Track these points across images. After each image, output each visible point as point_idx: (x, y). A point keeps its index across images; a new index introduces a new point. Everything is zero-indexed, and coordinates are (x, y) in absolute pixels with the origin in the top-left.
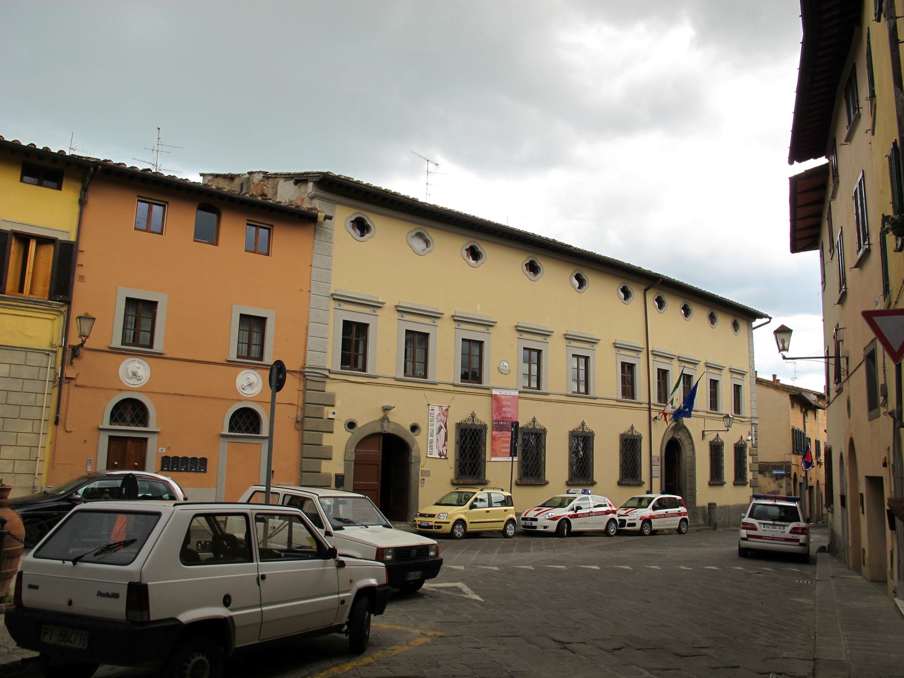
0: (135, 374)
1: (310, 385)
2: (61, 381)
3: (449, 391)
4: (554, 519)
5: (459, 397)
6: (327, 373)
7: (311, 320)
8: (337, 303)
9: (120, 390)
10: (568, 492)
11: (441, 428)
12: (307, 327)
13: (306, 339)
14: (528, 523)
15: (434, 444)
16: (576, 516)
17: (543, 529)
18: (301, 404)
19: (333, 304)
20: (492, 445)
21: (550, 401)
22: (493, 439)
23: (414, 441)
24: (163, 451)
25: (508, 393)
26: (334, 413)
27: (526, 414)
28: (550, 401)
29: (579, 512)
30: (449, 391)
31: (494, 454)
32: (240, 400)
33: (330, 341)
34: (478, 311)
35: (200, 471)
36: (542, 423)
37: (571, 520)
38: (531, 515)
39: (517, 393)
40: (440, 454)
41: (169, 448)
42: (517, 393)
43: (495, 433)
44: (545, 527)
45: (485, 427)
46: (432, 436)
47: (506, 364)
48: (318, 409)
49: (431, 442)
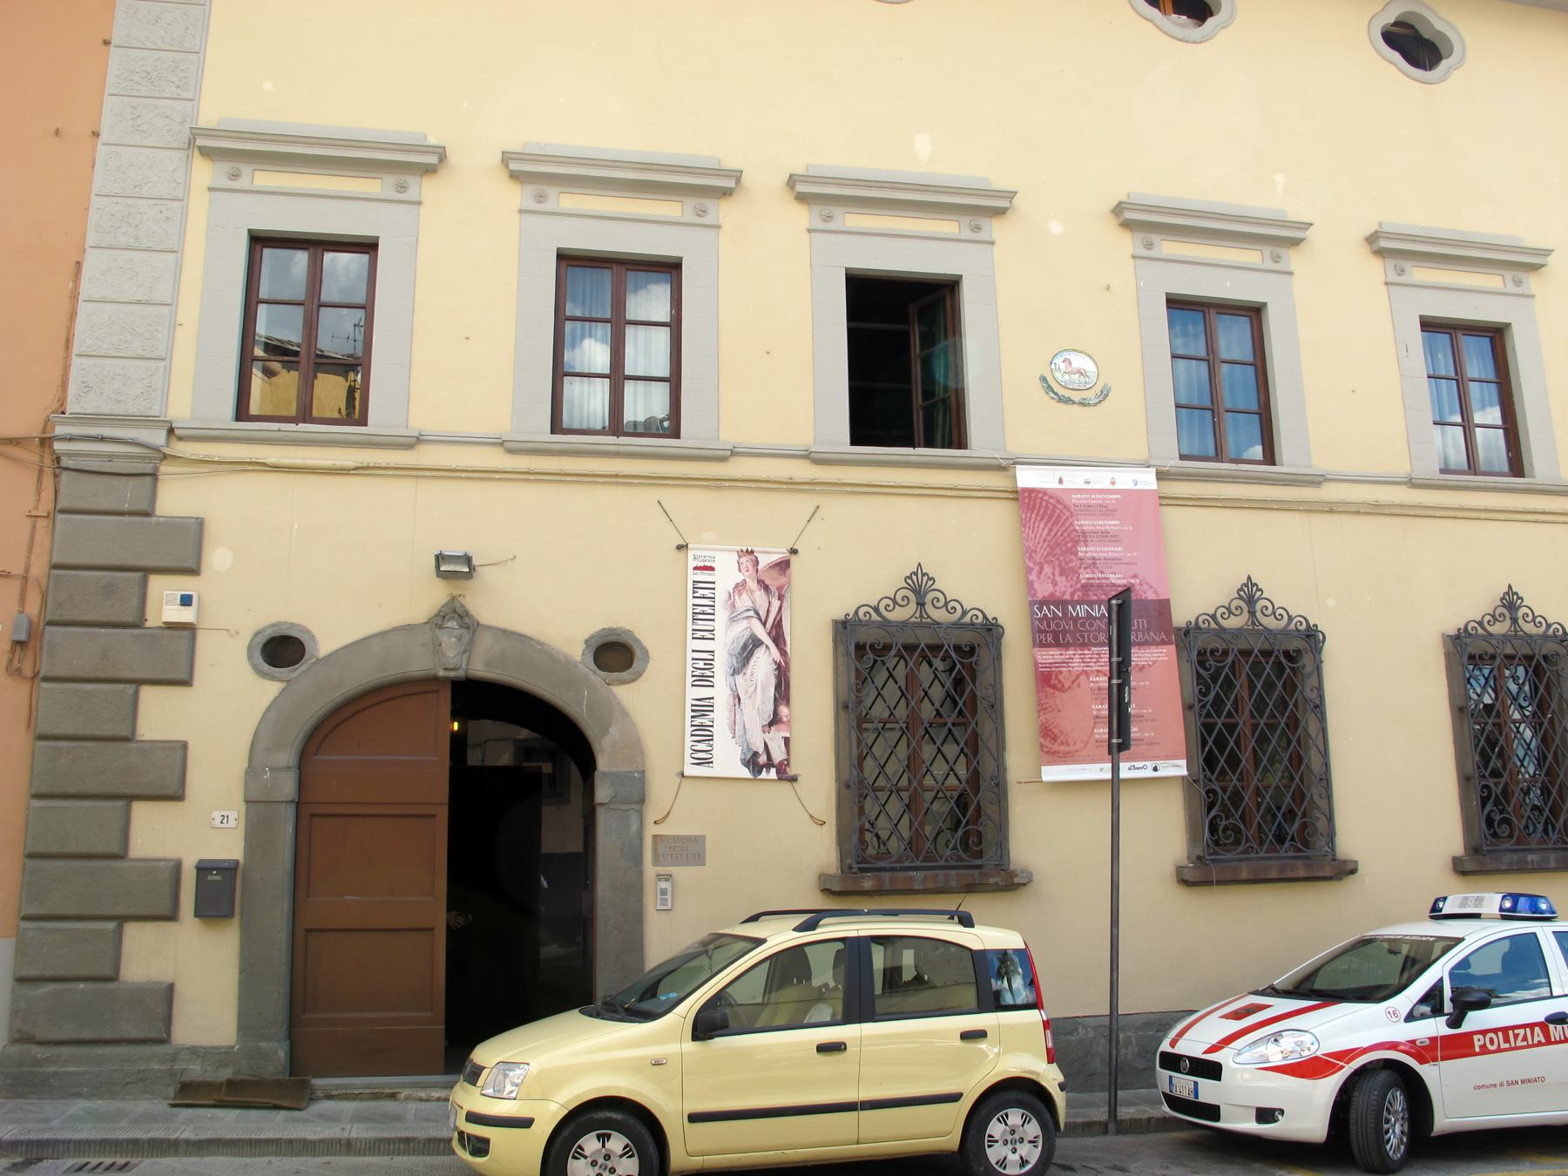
1: (75, 491)
3: (791, 485)
4: (1312, 1068)
5: (838, 510)
6: (158, 437)
7: (92, 238)
10: (1436, 914)
11: (749, 648)
12: (79, 264)
13: (73, 314)
14: (1183, 1084)
15: (720, 717)
16: (1457, 1047)
17: (1250, 1126)
18: (39, 569)
19: (204, 173)
20: (1042, 708)
21: (1331, 509)
22: (1046, 680)
23: (611, 712)
25: (1100, 479)
26: (186, 601)
27: (1208, 562)
28: (1331, 509)
29: (1475, 1020)
30: (791, 485)
31: (1053, 745)
33: (189, 310)
34: (924, 157)
36: (1293, 596)
37: (1427, 1072)
38: (1193, 1045)
39: (1147, 480)
40: (753, 763)
42: (1147, 480)
43: (1050, 656)
44: (1265, 1115)
45: (991, 630)
46: (703, 679)
47: (1079, 362)
48: (109, 590)
49: (703, 708)
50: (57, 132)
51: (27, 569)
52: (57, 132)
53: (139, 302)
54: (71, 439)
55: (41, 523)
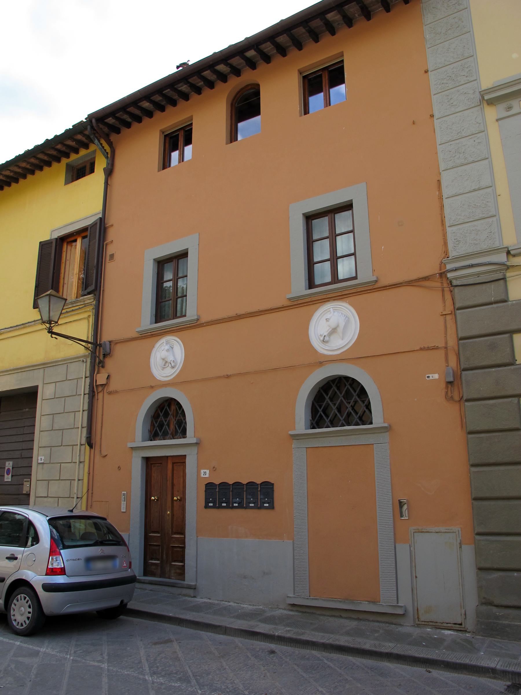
0: (167, 358)
1: (464, 297)
2: (93, 393)
6: (502, 258)
8: (502, 107)
9: (152, 387)
12: (439, 181)
13: (442, 207)
18: (452, 342)
19: (491, 113)
24: (205, 473)
32: (321, 364)
35: (261, 507)
41: (214, 469)
50: (414, 123)
51: (446, 343)
52: (414, 123)
53: (475, 190)
54: (456, 270)
55: (448, 318)
